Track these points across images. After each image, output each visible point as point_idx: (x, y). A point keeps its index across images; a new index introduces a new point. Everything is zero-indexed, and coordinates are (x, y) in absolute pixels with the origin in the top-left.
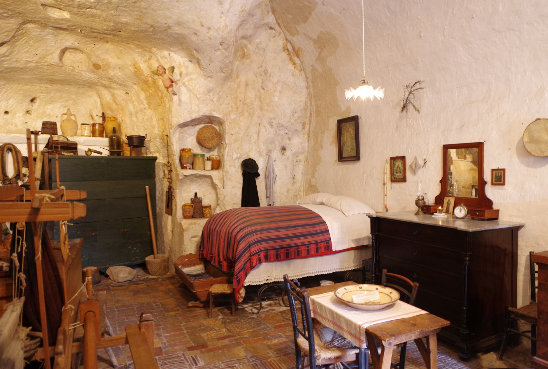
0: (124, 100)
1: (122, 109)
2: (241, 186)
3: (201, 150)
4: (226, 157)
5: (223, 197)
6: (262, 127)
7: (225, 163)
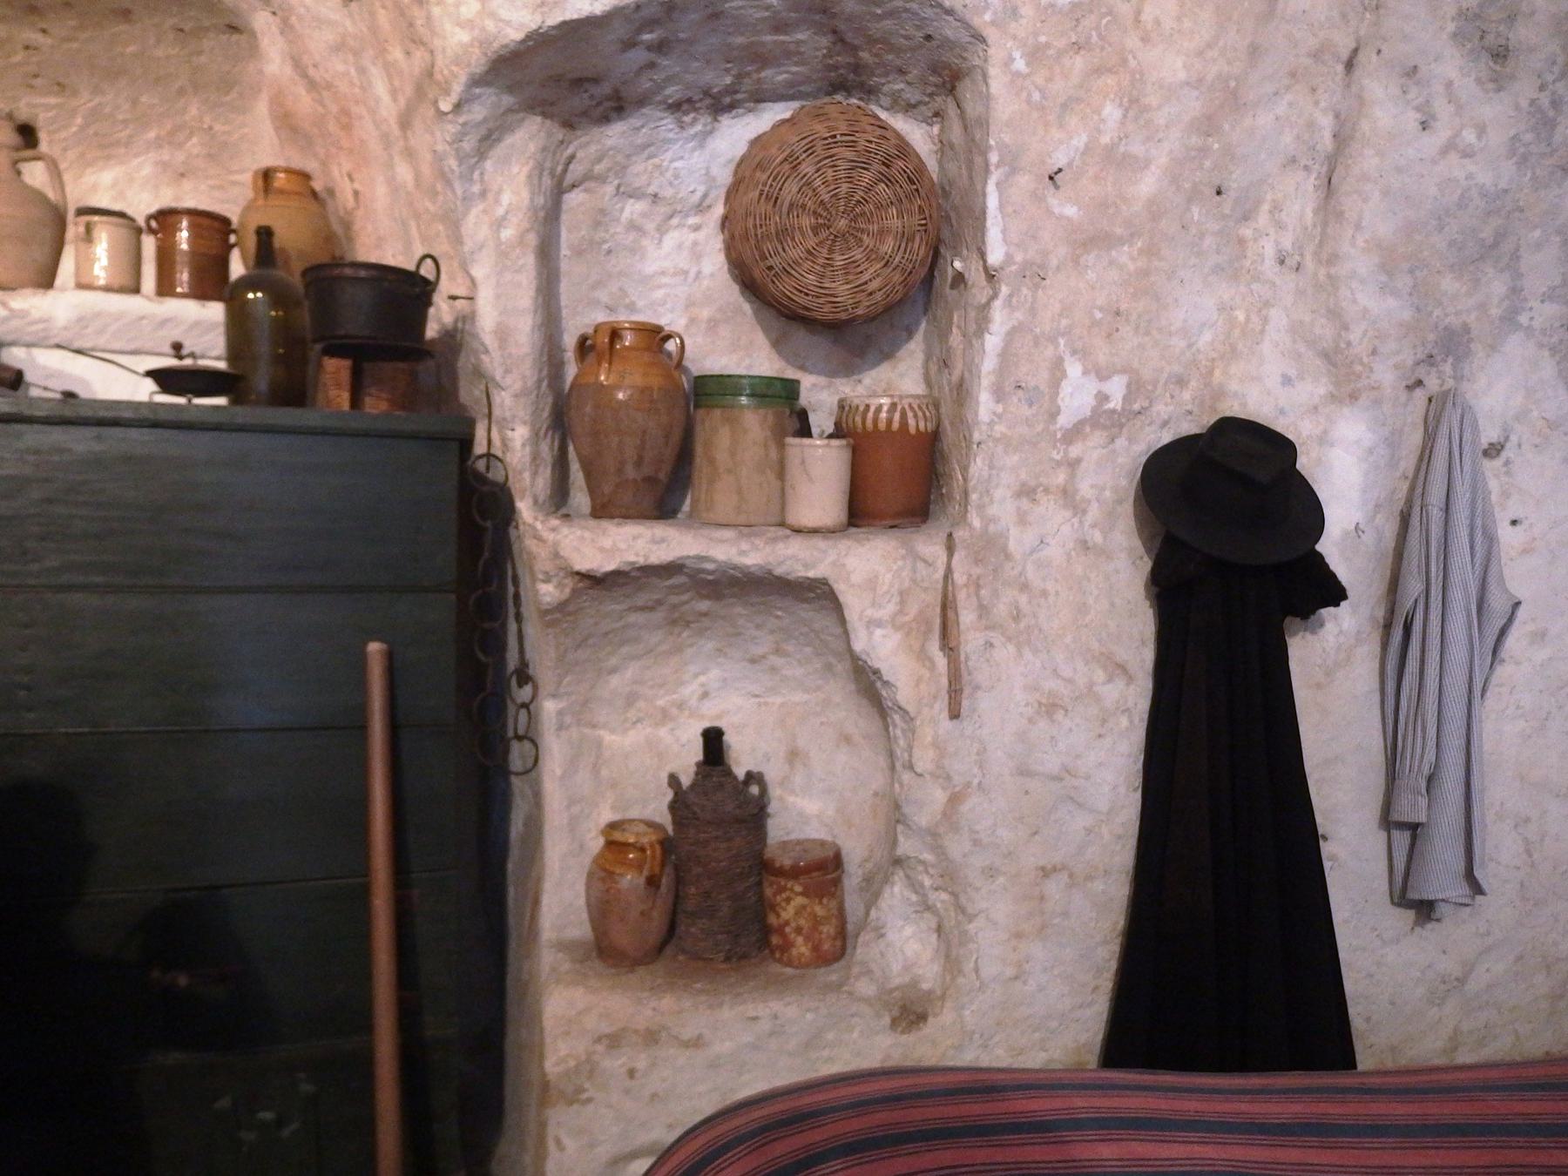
0: (339, 47)
1: (346, 121)
2: (1129, 699)
3: (778, 344)
4: (985, 405)
5: (939, 796)
6: (1377, 87)
7: (978, 467)
